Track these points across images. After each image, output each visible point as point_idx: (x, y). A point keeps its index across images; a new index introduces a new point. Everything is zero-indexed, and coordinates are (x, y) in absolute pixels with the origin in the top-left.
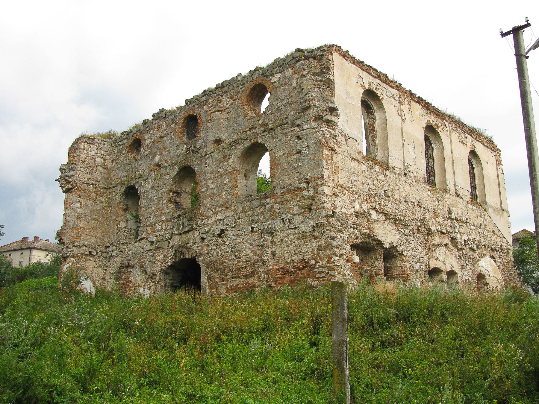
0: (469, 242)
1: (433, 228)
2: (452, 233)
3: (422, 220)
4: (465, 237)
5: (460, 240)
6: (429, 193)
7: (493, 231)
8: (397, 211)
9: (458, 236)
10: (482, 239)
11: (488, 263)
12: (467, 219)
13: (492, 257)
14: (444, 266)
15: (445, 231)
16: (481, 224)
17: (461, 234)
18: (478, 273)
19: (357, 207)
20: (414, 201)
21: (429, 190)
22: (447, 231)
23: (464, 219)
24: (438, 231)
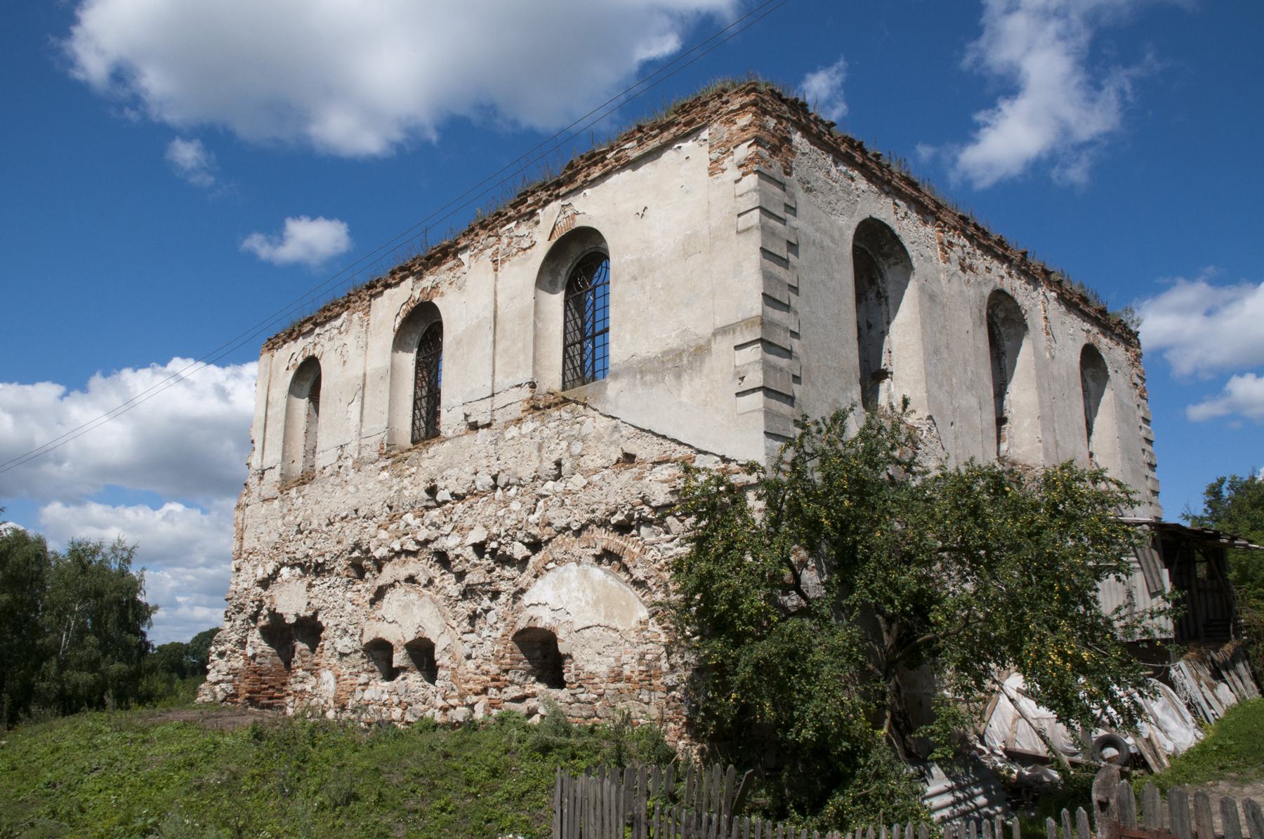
0: (494, 545)
1: (377, 554)
2: (436, 539)
3: (357, 546)
4: (477, 536)
5: (458, 551)
6: (385, 474)
7: (629, 458)
8: (311, 552)
9: (450, 543)
10: (550, 514)
11: (574, 585)
12: (495, 478)
13: (607, 556)
14: (400, 630)
15: (411, 546)
16: (558, 464)
17: (459, 529)
18: (521, 625)
19: (261, 573)
20: (344, 514)
21: (383, 468)
22: (418, 542)
23: (484, 481)
24: (398, 554)
